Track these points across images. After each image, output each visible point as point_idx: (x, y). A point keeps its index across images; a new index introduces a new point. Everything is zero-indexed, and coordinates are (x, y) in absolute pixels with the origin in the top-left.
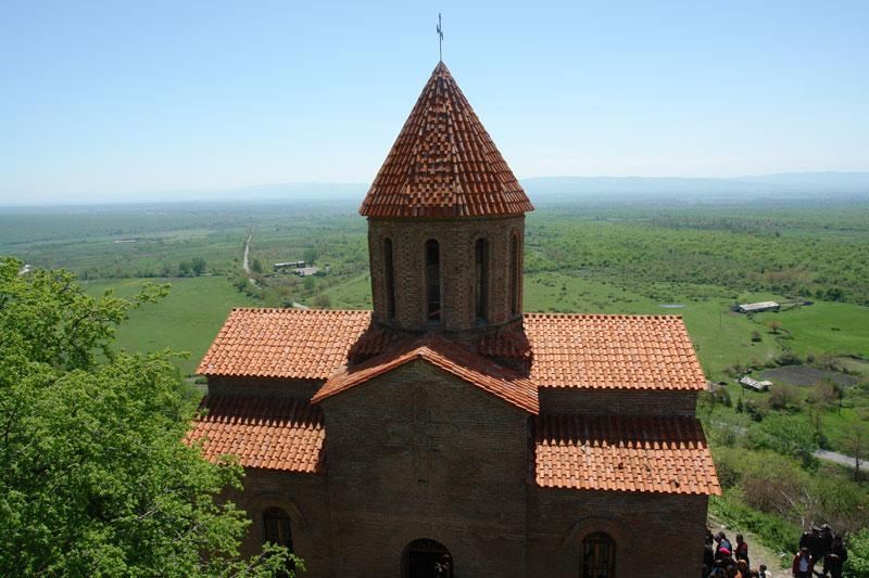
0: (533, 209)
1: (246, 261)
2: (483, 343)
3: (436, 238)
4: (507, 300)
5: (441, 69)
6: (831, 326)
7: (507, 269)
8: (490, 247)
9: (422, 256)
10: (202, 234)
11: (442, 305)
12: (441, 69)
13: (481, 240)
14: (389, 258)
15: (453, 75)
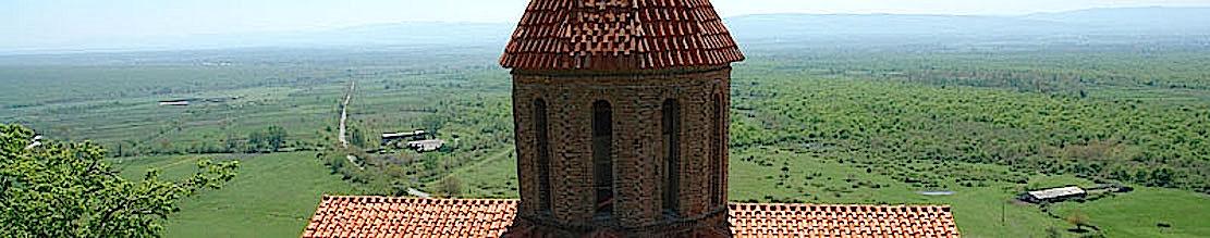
1: (343, 130)
4: (705, 185)
6: (1157, 222)
9: (587, 124)
10: (283, 92)
11: (615, 191)
13: (669, 101)
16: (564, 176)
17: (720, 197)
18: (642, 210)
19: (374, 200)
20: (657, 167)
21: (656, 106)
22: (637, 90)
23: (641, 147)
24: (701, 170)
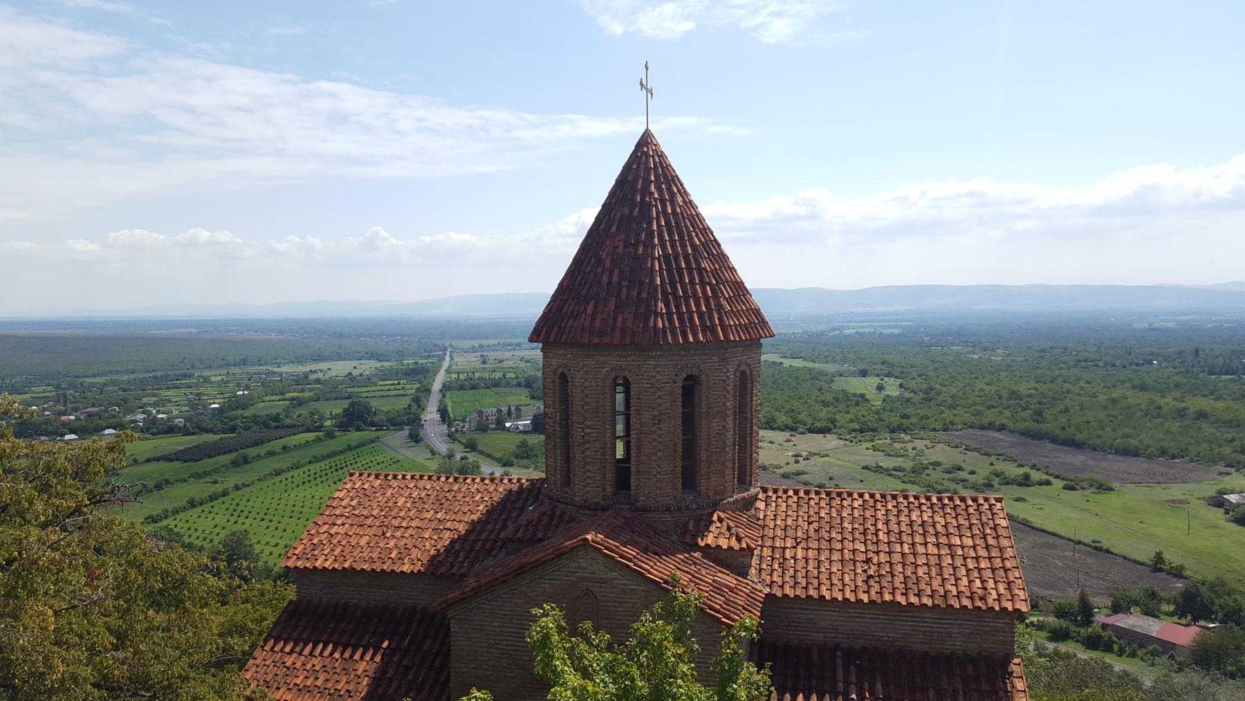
0: (772, 335)
5: (646, 140)
6: (1197, 496)
7: (730, 420)
11: (633, 469)
12: (646, 140)
13: (690, 378)
15: (665, 148)
17: (748, 477)
21: (675, 383)
22: (656, 366)
23: (659, 424)
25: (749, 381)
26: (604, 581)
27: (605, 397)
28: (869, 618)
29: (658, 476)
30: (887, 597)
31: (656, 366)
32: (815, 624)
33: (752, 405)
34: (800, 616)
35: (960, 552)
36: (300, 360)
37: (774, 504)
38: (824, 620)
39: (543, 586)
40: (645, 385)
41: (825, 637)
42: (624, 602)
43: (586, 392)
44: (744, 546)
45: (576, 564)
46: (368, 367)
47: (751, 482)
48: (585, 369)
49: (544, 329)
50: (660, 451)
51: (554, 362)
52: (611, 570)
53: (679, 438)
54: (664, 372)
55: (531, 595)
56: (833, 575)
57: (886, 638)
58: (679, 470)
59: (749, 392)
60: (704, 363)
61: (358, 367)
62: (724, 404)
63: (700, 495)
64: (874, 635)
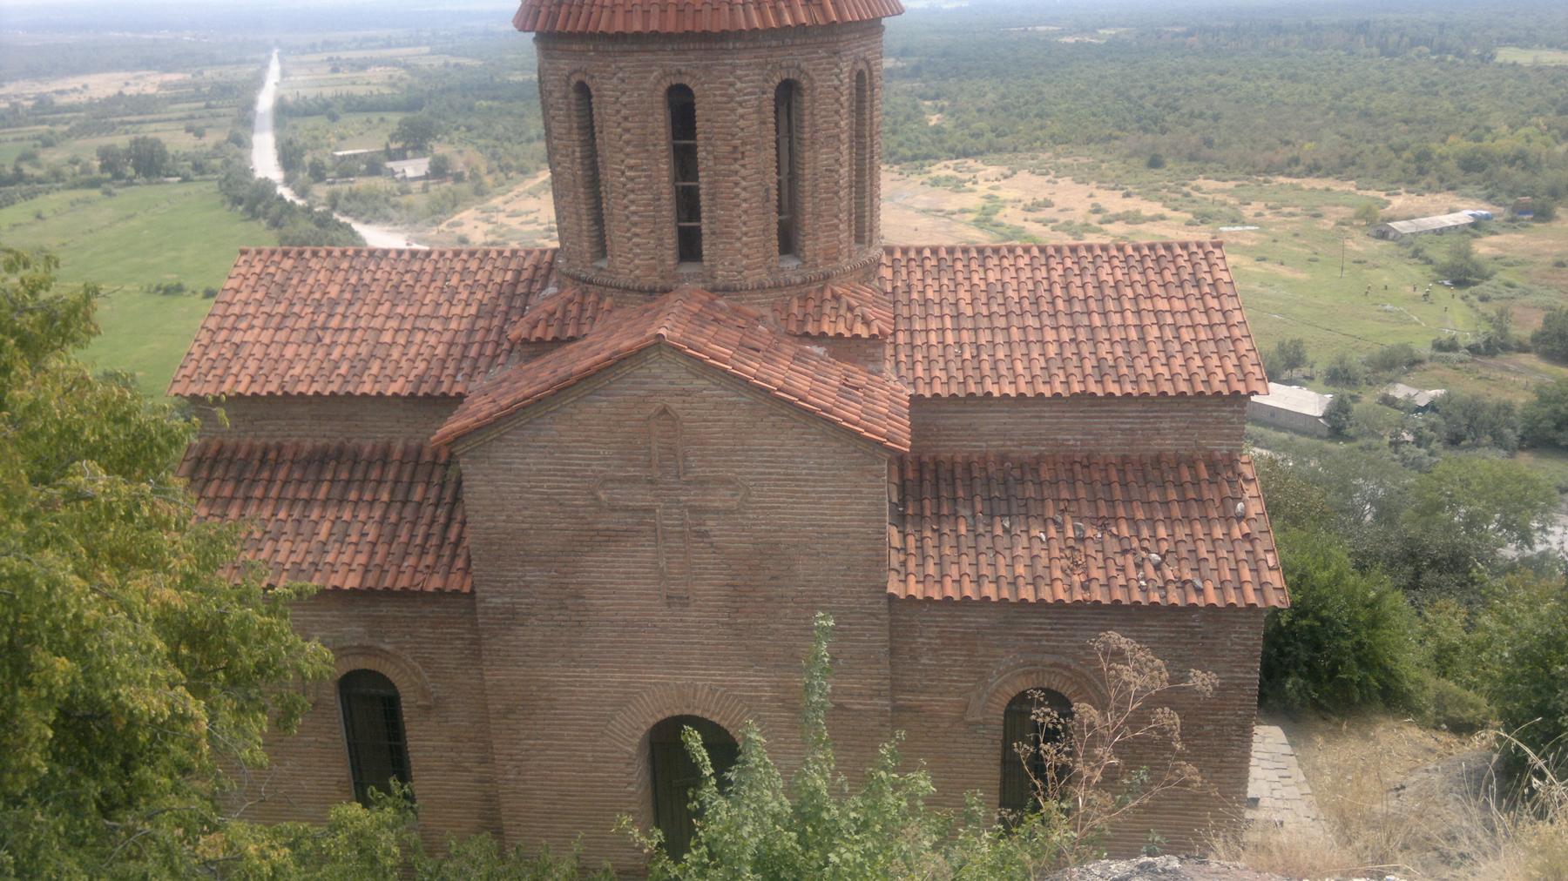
2: (795, 309)
3: (686, 81)
7: (844, 148)
8: (806, 98)
9: (660, 122)
11: (705, 230)
14: (588, 130)
16: (626, 207)
17: (867, 234)
18: (747, 257)
19: (323, 254)
20: (767, 190)
21: (764, 93)
24: (836, 193)
25: (868, 87)
26: (687, 393)
27: (656, 120)
28: (1051, 417)
29: (745, 239)
30: (1077, 388)
31: (734, 67)
32: (975, 430)
33: (872, 124)
34: (956, 421)
35: (1169, 320)
36: (34, 73)
37: (904, 271)
38: (988, 424)
39: (598, 404)
40: (718, 99)
41: (988, 446)
42: (720, 420)
43: (624, 112)
44: (876, 331)
45: (645, 371)
46: (149, 84)
47: (871, 241)
48: (620, 75)
49: (543, 9)
50: (745, 200)
51: (565, 65)
52: (697, 377)
53: (772, 179)
54: (747, 75)
55: (579, 417)
56: (999, 364)
57: (1071, 443)
58: (774, 227)
59: (867, 104)
60: (807, 60)
61: (132, 82)
62: (837, 124)
63: (805, 263)
64: (1056, 440)
